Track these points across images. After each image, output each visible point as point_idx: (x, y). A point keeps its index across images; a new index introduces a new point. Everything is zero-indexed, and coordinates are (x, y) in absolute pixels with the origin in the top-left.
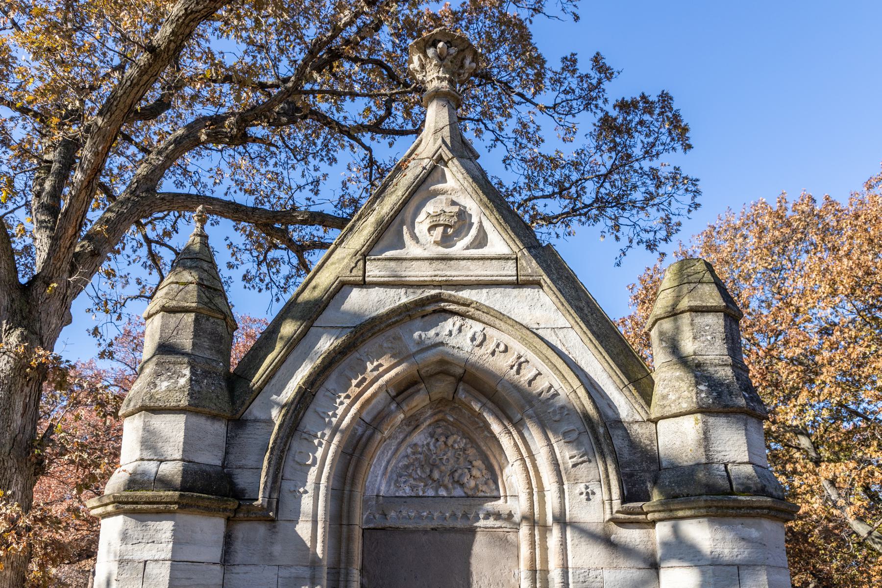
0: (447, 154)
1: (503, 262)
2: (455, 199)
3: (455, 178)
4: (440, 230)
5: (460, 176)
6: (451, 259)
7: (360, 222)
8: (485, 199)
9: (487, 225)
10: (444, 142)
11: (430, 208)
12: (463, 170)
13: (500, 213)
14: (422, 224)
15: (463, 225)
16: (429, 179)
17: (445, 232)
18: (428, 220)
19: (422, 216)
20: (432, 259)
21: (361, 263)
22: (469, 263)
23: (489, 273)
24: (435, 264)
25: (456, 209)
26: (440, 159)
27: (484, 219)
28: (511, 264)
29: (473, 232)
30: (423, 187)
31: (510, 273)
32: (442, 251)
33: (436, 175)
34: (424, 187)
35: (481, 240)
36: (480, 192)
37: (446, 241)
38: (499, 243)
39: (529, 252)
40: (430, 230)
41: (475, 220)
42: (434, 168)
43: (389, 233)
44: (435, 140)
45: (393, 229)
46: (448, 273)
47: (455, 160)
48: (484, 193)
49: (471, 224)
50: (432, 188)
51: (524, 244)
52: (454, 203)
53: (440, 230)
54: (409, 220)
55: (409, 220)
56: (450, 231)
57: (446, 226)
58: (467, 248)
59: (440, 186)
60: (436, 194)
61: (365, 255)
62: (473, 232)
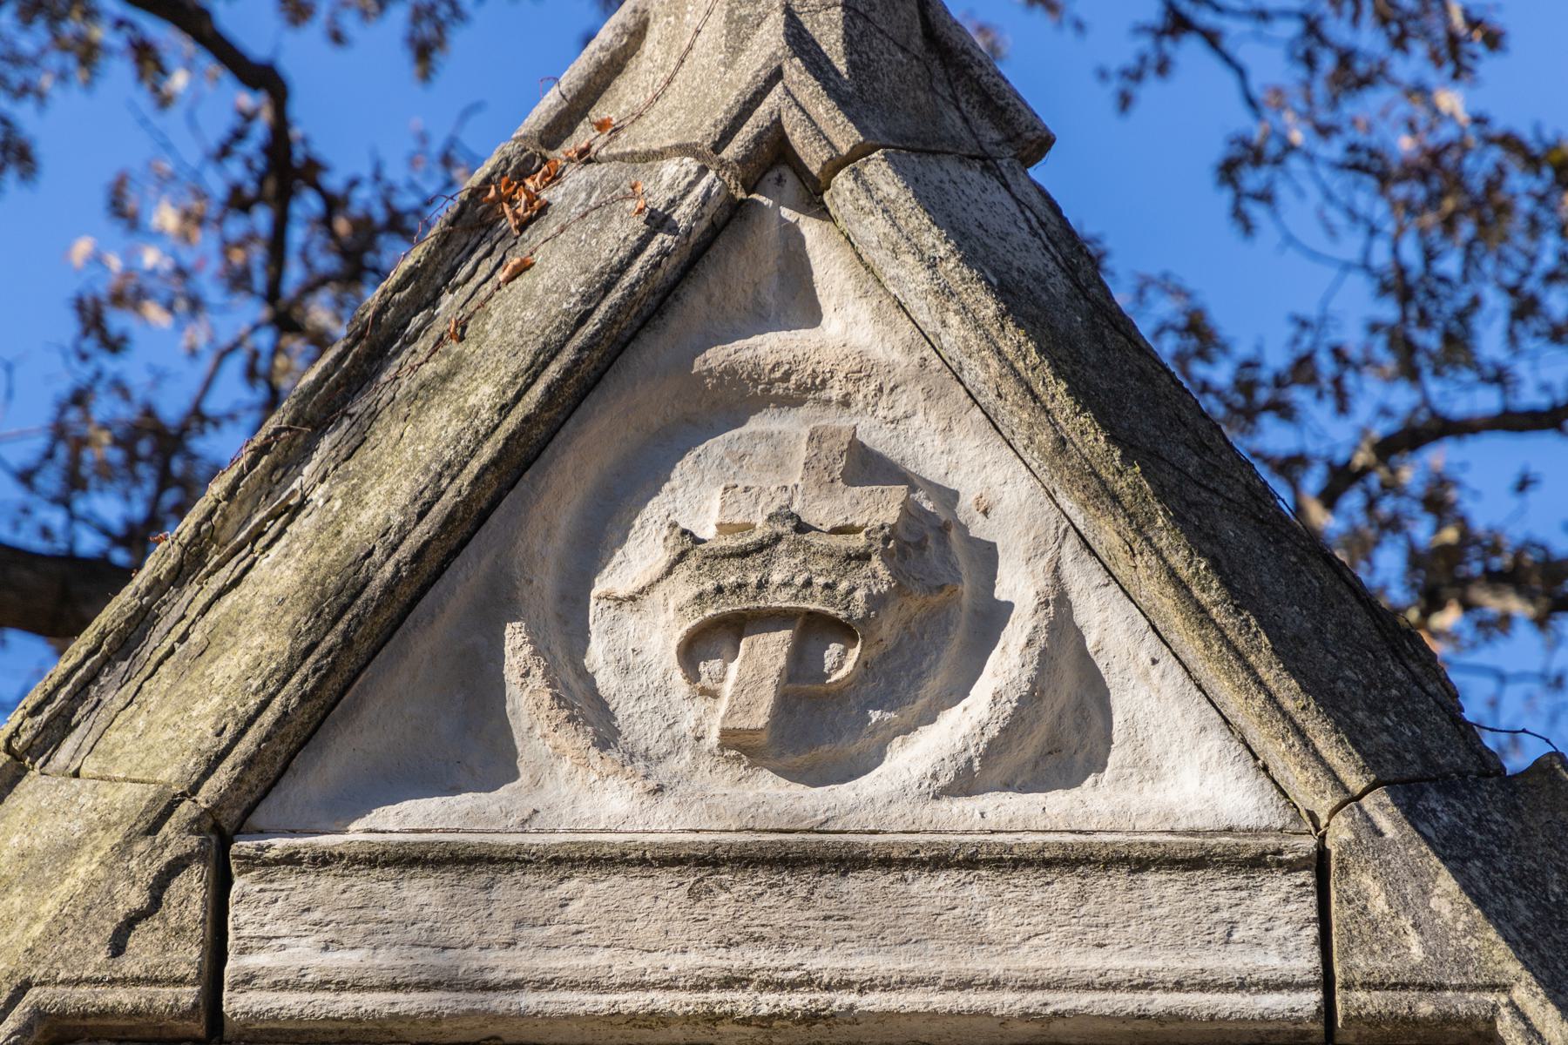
0: (818, 125)
1: (1219, 889)
2: (877, 437)
3: (873, 297)
4: (769, 651)
5: (911, 279)
6: (848, 862)
7: (195, 594)
8: (1092, 441)
9: (1106, 623)
10: (799, 39)
11: (700, 497)
12: (933, 240)
13: (1201, 538)
14: (639, 613)
15: (934, 625)
16: (695, 300)
17: (801, 665)
18: (682, 589)
19: (639, 557)
20: (708, 861)
21: (191, 888)
22: (978, 890)
23: (1119, 963)
24: (732, 897)
25: (880, 508)
26: (774, 155)
27: (1082, 580)
28: (1280, 902)
29: (1007, 666)
30: (658, 345)
31: (1270, 962)
32: (777, 800)
33: (746, 268)
34: (654, 350)
35: (1064, 729)
36: (1057, 394)
37: (811, 730)
38: (1190, 752)
39: (1412, 813)
40: (698, 647)
41: (1018, 584)
42: (728, 220)
43: (404, 669)
44: (738, 32)
45: (427, 641)
46: (826, 963)
47: (877, 169)
48: (1083, 395)
49: (993, 617)
50: (715, 357)
51: (1371, 760)
52: (867, 466)
53: (769, 651)
54: (544, 582)
55: (544, 582)
56: (841, 662)
57: (814, 629)
58: (965, 783)
59: (769, 347)
60: (739, 399)
61: (223, 829)
62: (1007, 666)
